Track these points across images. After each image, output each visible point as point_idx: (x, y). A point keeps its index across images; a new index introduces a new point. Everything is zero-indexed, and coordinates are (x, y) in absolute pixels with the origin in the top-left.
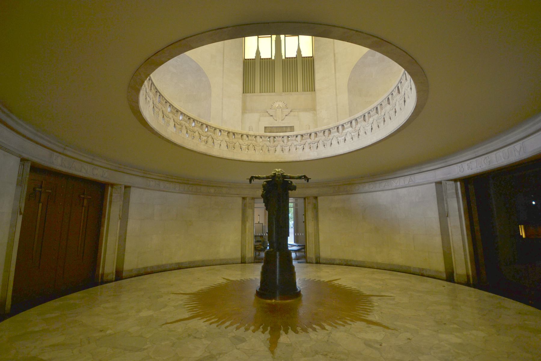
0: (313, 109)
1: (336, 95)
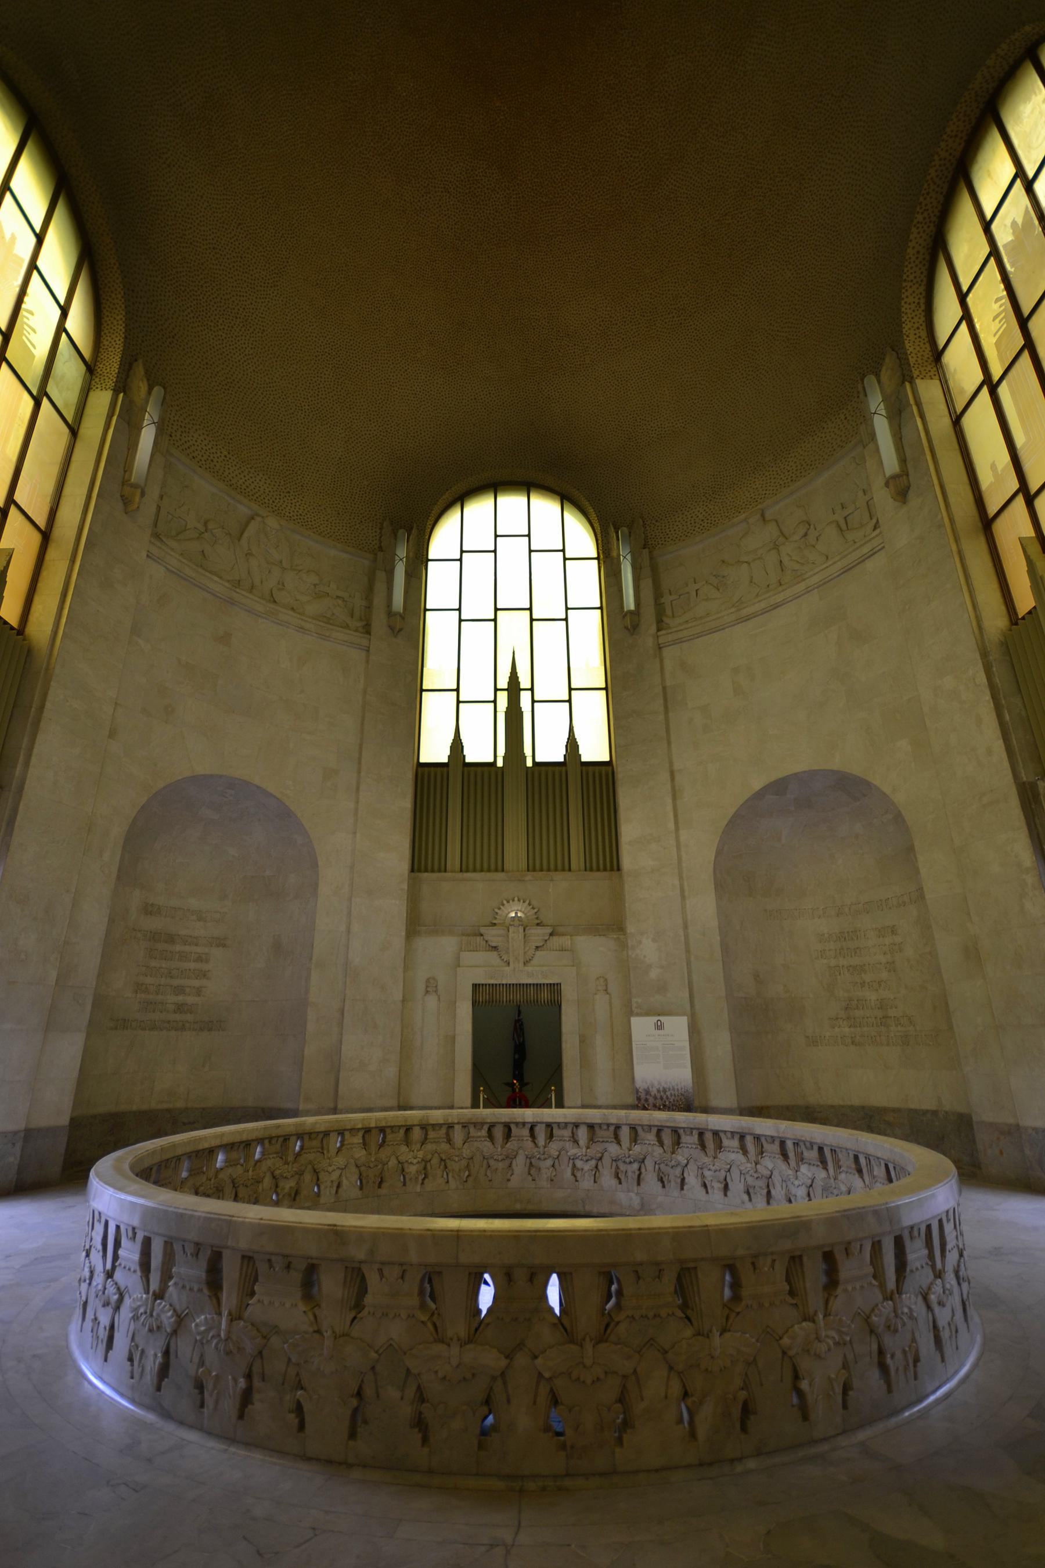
0: (613, 925)
1: (683, 897)
